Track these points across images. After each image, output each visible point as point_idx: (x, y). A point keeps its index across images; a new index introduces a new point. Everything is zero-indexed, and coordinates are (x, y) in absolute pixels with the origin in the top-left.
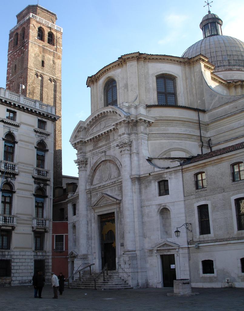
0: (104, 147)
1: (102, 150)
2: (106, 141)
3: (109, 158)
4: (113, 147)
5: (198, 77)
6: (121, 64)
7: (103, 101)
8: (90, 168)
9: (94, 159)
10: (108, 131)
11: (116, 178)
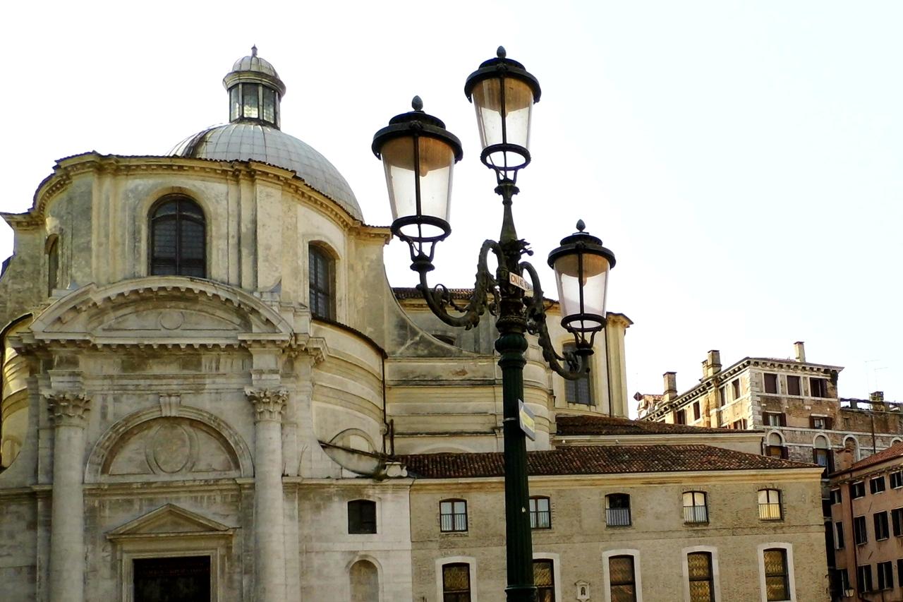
0: (175, 382)
1: (164, 387)
2: (185, 366)
3: (195, 415)
4: (215, 391)
6: (231, 173)
7: (144, 246)
8: (101, 424)
9: (120, 402)
10: (203, 346)
11: (214, 470)
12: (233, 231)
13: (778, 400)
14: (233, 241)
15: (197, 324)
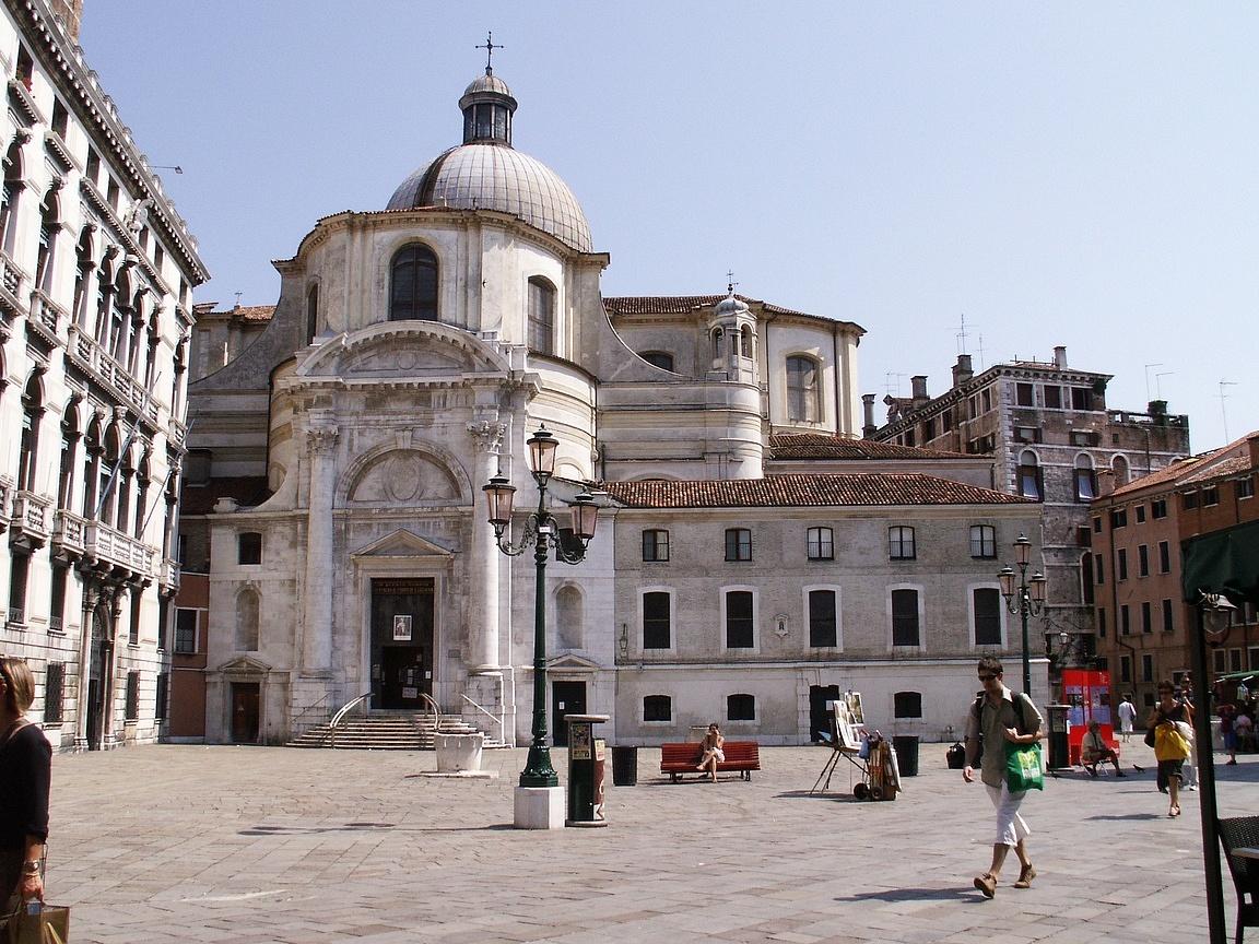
0: (409, 417)
1: (400, 422)
5: (590, 300)
12: (461, 274)
13: (1034, 413)
14: (461, 284)
15: (428, 363)
